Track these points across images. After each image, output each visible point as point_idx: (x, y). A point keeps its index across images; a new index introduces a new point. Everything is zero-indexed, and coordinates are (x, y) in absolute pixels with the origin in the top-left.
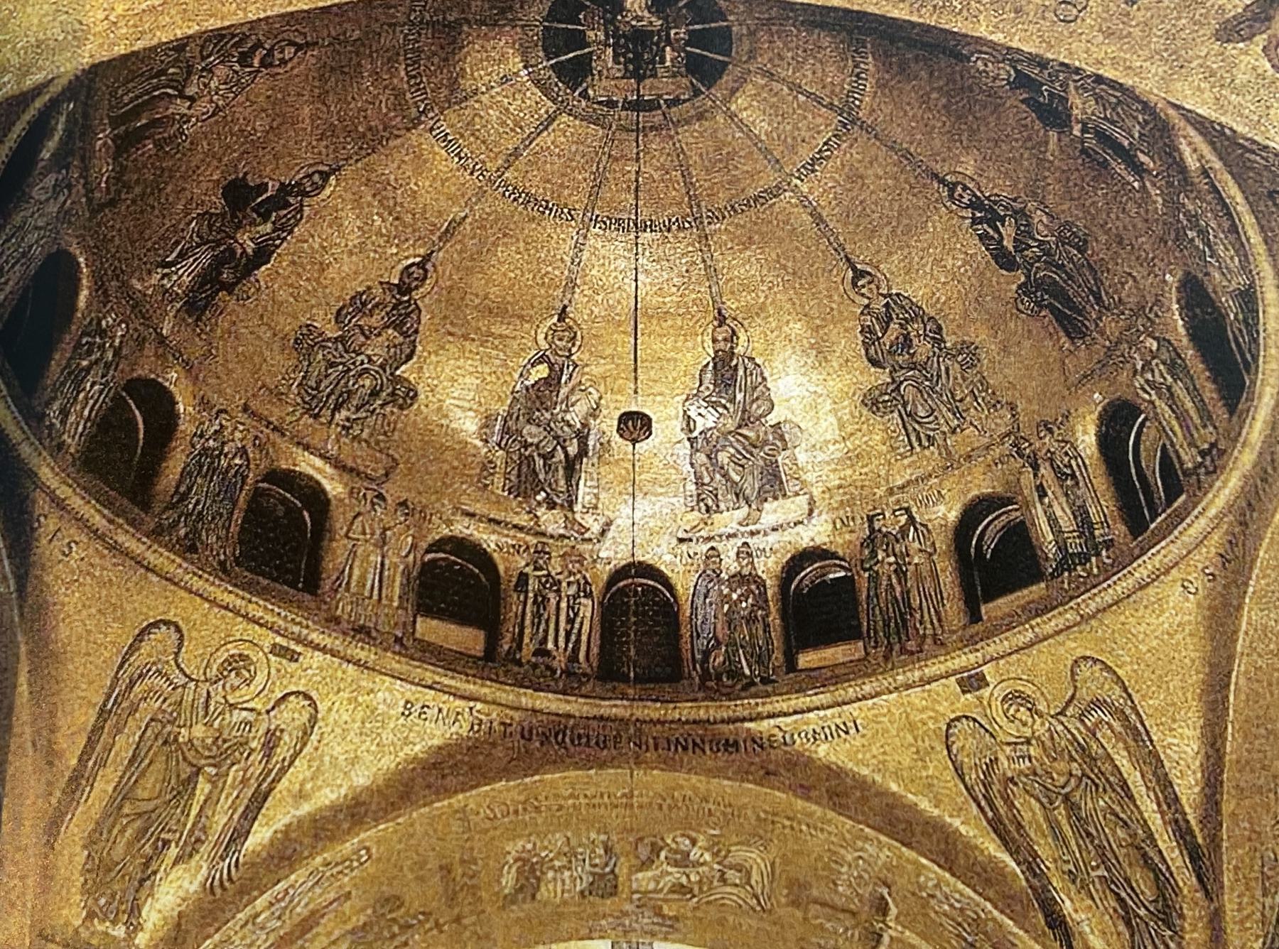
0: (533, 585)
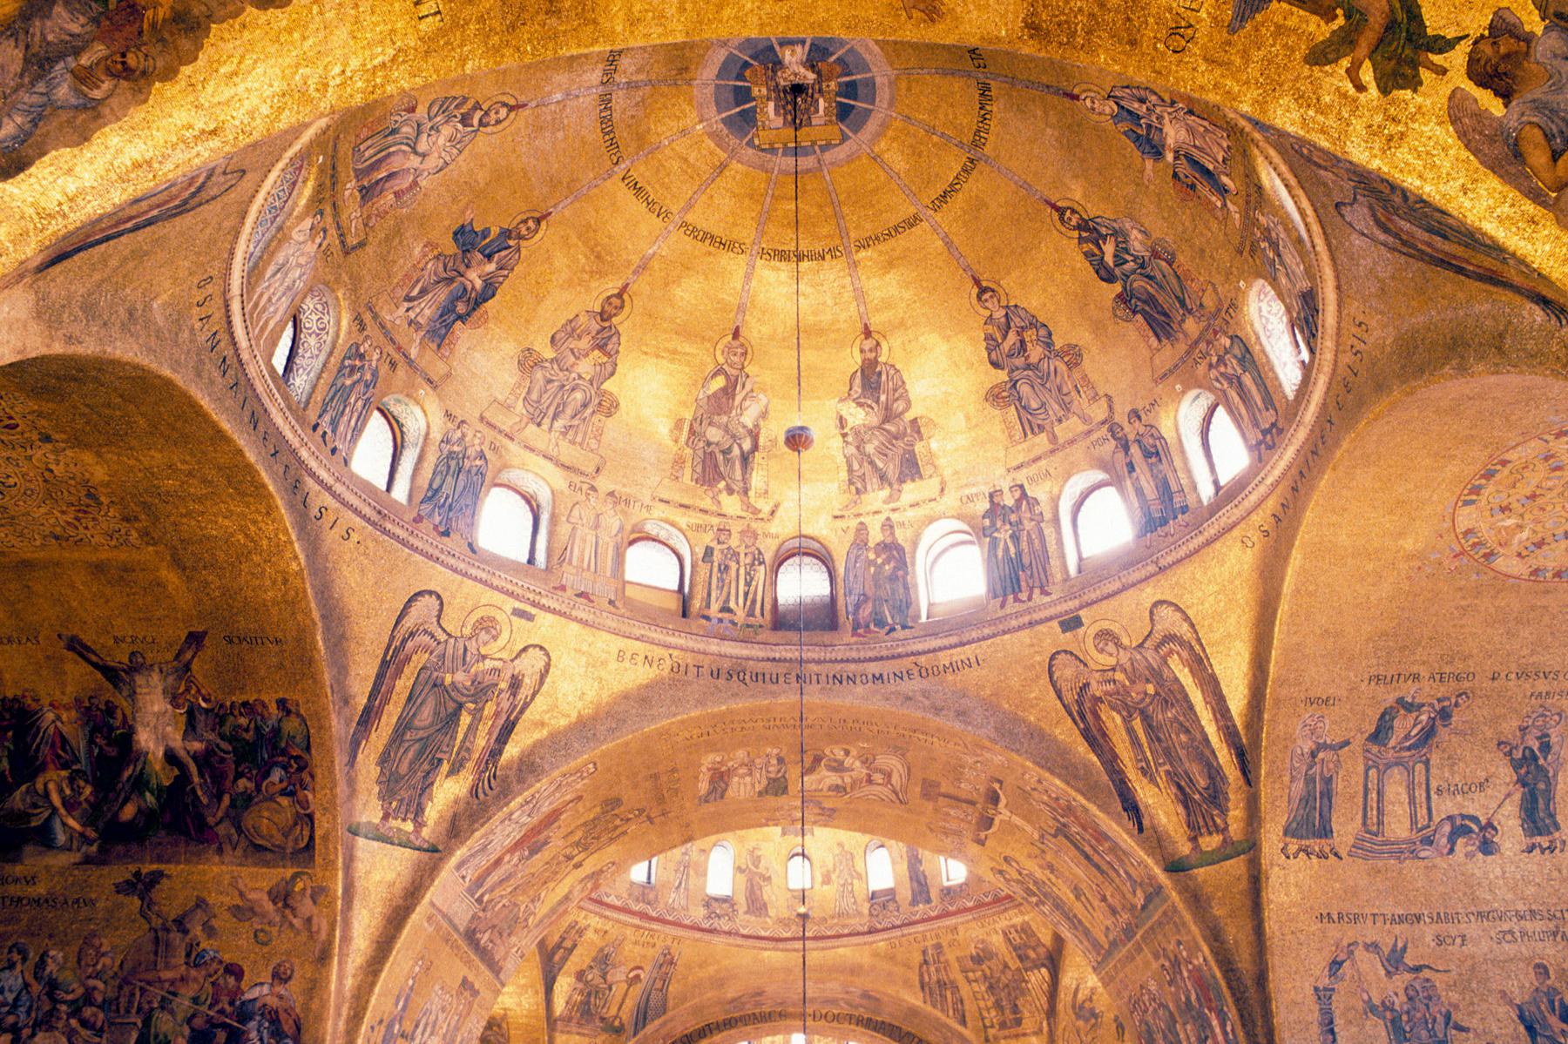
0: (717, 557)
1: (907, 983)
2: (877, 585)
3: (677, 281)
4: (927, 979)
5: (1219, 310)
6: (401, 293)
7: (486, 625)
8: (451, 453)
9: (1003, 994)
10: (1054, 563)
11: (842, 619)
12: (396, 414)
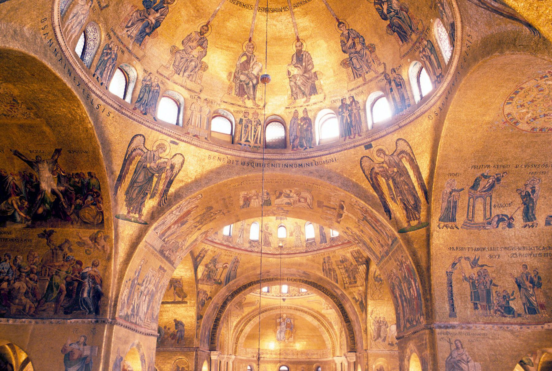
0: (244, 122)
2: (301, 132)
3: (228, 20)
5: (424, 31)
6: (124, 25)
7: (161, 147)
8: (146, 85)
10: (363, 125)
11: (288, 145)
12: (126, 70)
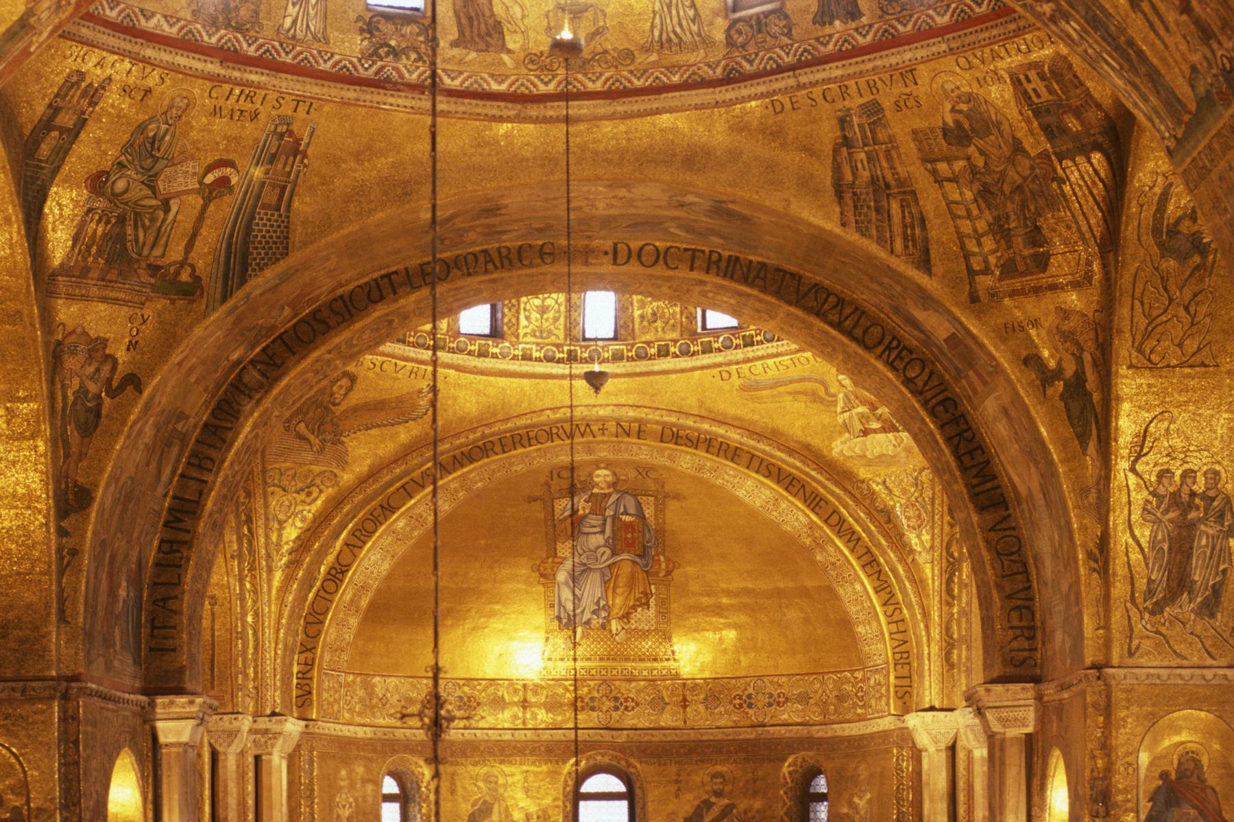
1: (806, 185)
4: (849, 177)
9: (1010, 207)
